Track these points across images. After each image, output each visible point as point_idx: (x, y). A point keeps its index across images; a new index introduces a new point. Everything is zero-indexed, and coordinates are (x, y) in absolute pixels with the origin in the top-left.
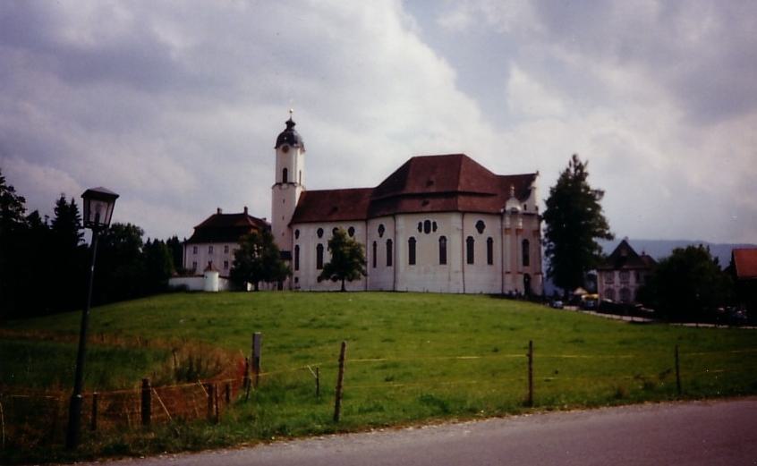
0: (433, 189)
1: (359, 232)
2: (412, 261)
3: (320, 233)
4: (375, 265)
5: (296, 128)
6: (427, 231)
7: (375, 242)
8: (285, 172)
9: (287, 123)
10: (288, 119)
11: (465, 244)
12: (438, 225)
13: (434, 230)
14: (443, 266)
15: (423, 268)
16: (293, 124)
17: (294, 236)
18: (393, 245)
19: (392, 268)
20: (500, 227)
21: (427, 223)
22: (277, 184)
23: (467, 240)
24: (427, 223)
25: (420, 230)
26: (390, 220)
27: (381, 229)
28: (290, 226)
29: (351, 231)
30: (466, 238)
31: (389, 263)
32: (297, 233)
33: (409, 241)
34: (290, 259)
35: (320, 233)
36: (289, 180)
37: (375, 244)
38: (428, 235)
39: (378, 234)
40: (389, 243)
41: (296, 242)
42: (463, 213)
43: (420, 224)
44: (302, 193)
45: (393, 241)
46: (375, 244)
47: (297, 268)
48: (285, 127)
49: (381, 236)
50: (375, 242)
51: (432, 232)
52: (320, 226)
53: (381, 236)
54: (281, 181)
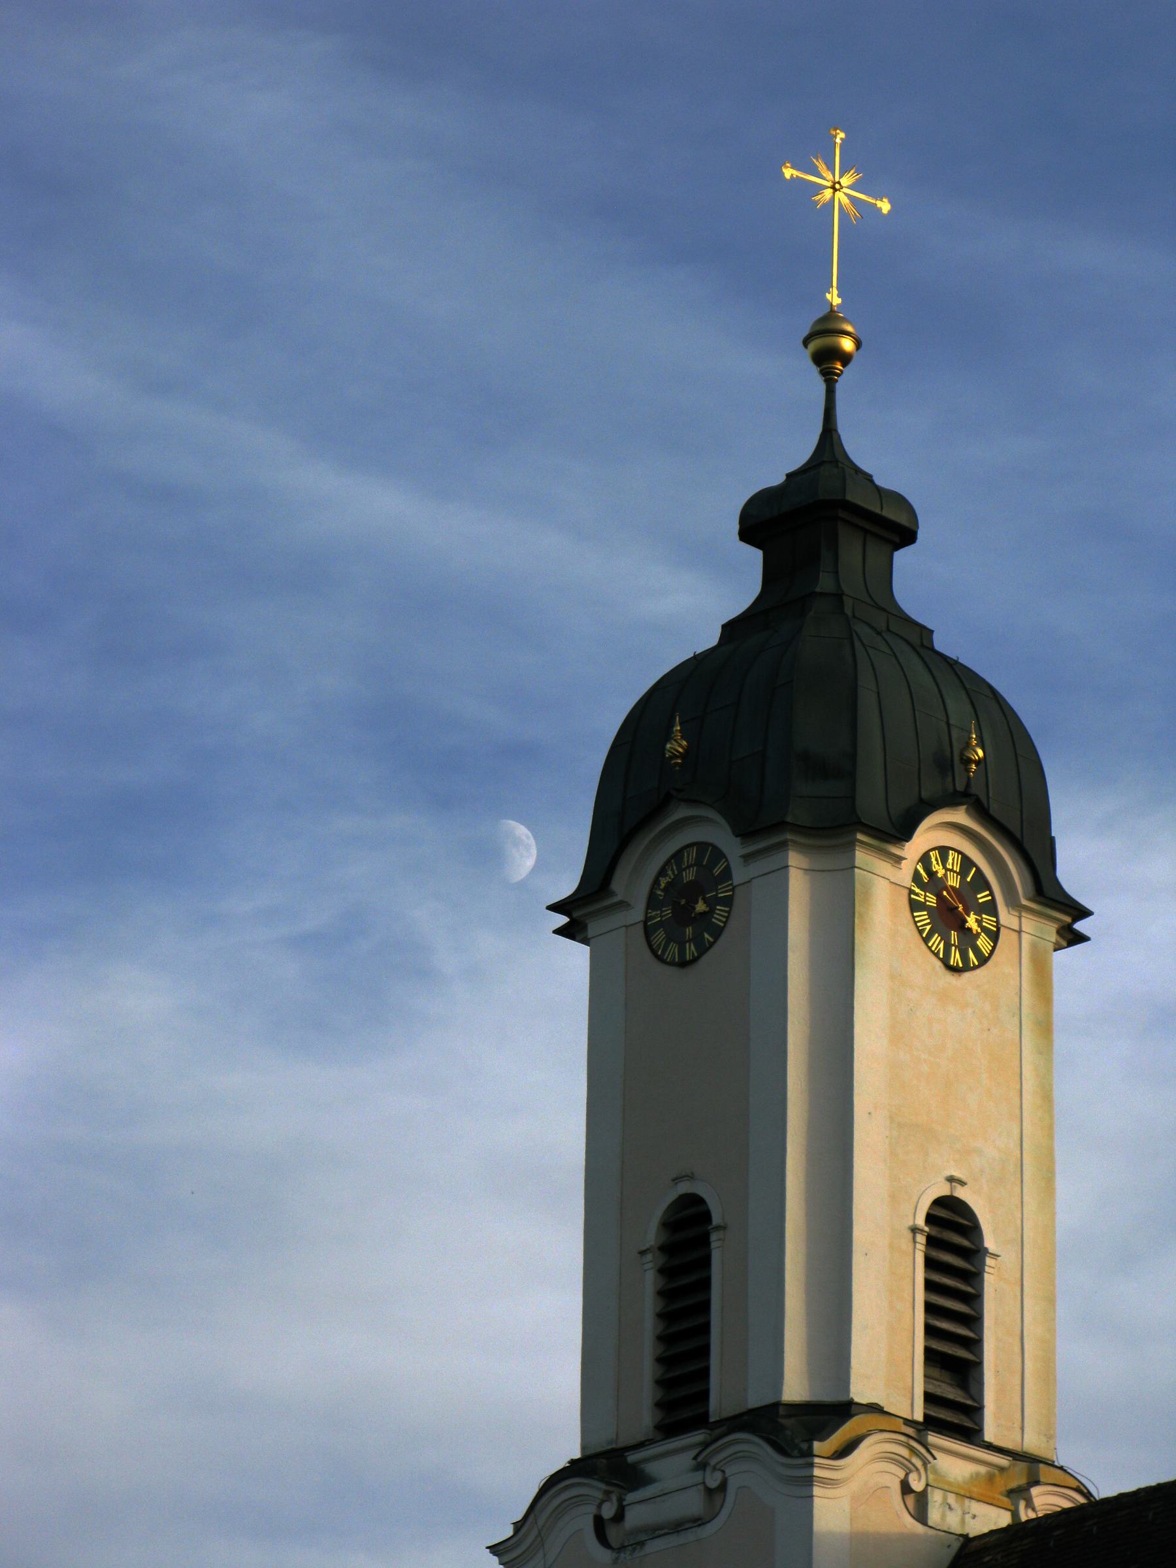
16: (907, 536)
54: (645, 1419)
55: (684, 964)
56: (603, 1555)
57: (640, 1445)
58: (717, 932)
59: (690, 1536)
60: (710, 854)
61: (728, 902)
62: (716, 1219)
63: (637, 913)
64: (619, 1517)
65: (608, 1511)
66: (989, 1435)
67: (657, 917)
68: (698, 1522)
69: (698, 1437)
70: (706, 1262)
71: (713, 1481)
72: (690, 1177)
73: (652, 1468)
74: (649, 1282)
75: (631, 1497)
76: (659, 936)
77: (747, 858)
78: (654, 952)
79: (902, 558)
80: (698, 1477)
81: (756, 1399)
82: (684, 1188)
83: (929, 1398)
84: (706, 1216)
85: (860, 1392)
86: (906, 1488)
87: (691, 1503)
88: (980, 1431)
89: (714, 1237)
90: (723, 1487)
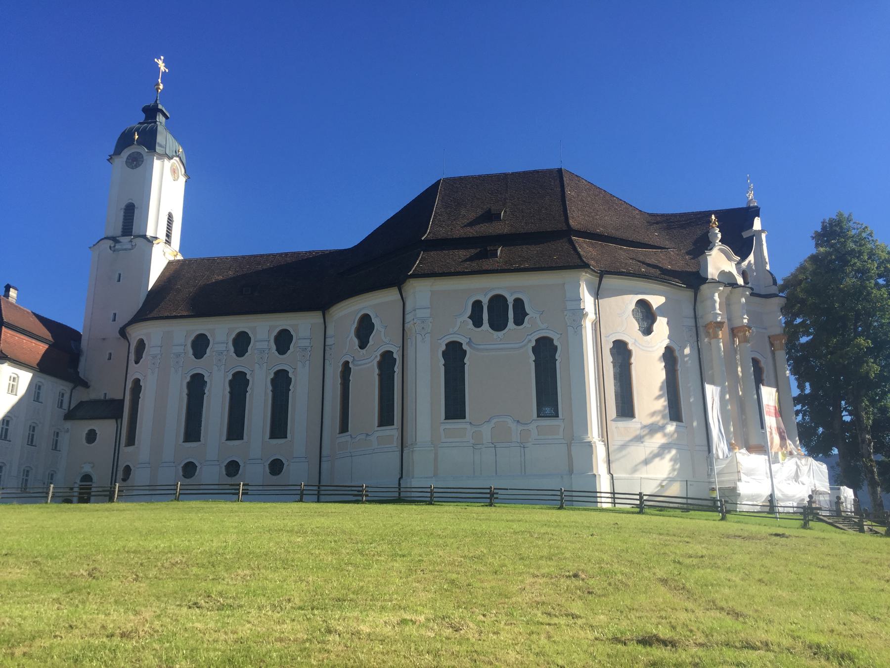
1: (306, 343)
3: (200, 345)
4: (344, 428)
6: (498, 324)
7: (346, 364)
11: (608, 359)
12: (528, 309)
13: (519, 321)
15: (486, 431)
17: (132, 357)
18: (397, 369)
19: (393, 432)
20: (691, 322)
24: (498, 302)
26: (390, 296)
27: (365, 329)
28: (123, 332)
29: (283, 341)
30: (607, 346)
31: (386, 419)
32: (141, 345)
33: (444, 354)
34: (118, 416)
35: (200, 345)
36: (135, 231)
37: (346, 369)
38: (500, 334)
39: (356, 341)
40: (387, 362)
41: (135, 371)
42: (602, 275)
43: (477, 305)
44: (170, 263)
46: (346, 369)
47: (131, 441)
48: (142, 117)
49: (363, 345)
50: (346, 365)
52: (201, 326)
53: (363, 345)
54: (119, 232)
56: (112, 252)
57: (119, 237)
60: (139, 154)
61: (143, 161)
62: (136, 206)
63: (125, 159)
64: (115, 246)
65: (112, 246)
67: (128, 161)
68: (130, 249)
72: (132, 199)
73: (121, 240)
74: (122, 213)
81: (141, 234)
82: (130, 201)
84: (134, 206)
85: (157, 236)
87: (130, 247)
89: (135, 210)
90: (136, 245)
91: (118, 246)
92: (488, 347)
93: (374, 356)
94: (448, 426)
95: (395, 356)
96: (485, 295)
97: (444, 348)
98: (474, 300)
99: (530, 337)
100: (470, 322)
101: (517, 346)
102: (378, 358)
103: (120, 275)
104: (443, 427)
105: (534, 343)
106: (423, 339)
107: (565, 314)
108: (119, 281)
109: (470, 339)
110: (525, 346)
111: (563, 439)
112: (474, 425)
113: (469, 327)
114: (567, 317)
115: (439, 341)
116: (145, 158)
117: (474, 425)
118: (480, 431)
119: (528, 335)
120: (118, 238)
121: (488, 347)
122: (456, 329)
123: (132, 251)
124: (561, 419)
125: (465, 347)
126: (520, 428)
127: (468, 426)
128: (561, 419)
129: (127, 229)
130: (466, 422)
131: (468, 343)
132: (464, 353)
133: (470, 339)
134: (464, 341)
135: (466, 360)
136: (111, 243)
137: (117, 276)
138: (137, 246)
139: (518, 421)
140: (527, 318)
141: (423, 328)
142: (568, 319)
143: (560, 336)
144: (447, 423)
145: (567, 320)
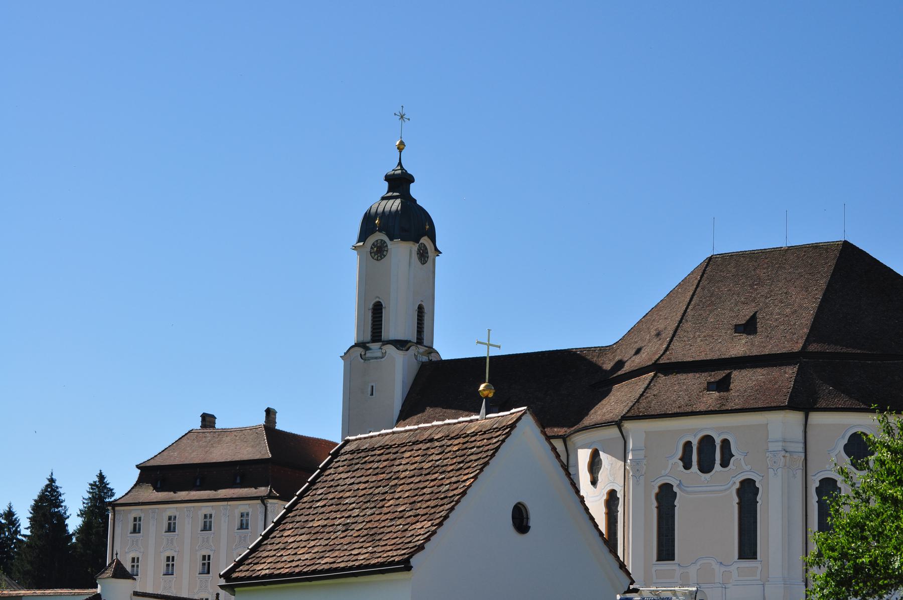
0: (740, 347)
2: (666, 551)
5: (415, 190)
6: (706, 467)
8: (377, 310)
9: (388, 178)
10: (391, 167)
11: (814, 498)
12: (734, 450)
13: (725, 464)
14: (747, 564)
18: (620, 509)
21: (707, 442)
22: (356, 345)
23: (818, 491)
25: (687, 466)
30: (814, 484)
33: (658, 496)
36: (385, 336)
38: (707, 476)
43: (688, 445)
45: (620, 495)
51: (717, 466)
54: (368, 337)
55: (377, 260)
57: (368, 343)
58: (385, 256)
59: (379, 360)
61: (387, 251)
64: (365, 354)
65: (363, 353)
66: (425, 344)
68: (382, 358)
69: (381, 343)
70: (382, 313)
71: (384, 351)
74: (370, 314)
75: (367, 352)
76: (373, 254)
77: (391, 244)
78: (372, 257)
79: (412, 185)
80: (381, 350)
82: (377, 300)
83: (417, 338)
84: (382, 305)
86: (415, 355)
87: (379, 354)
88: (423, 343)
90: (386, 352)
91: (369, 354)
92: (697, 489)
93: (602, 495)
94: (659, 568)
95: (618, 496)
96: (695, 436)
97: (656, 490)
98: (687, 440)
99: (734, 479)
100: (681, 463)
101: (723, 488)
102: (605, 497)
103: (373, 387)
104: (654, 569)
105: (737, 486)
106: (638, 481)
107: (767, 455)
108: (372, 394)
109: (680, 481)
110: (730, 488)
111: (760, 580)
112: (683, 567)
113: (679, 469)
114: (768, 459)
115: (653, 483)
116: (389, 247)
117: (683, 567)
118: (687, 572)
119: (733, 477)
120: (367, 345)
121: (697, 489)
122: (668, 470)
123: (383, 359)
124: (759, 561)
125: (675, 489)
126: (723, 569)
127: (676, 567)
128: (759, 561)
129: (376, 334)
130: (675, 564)
131: (678, 486)
132: (674, 495)
133: (680, 481)
134: (674, 483)
135: (676, 503)
136: (360, 350)
137: (370, 389)
138: (387, 354)
139: (721, 563)
140: (733, 459)
141: (638, 470)
142: (769, 460)
143: (761, 477)
144: (658, 564)
145: (768, 461)
